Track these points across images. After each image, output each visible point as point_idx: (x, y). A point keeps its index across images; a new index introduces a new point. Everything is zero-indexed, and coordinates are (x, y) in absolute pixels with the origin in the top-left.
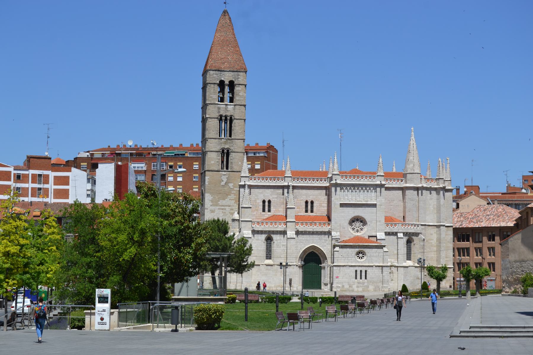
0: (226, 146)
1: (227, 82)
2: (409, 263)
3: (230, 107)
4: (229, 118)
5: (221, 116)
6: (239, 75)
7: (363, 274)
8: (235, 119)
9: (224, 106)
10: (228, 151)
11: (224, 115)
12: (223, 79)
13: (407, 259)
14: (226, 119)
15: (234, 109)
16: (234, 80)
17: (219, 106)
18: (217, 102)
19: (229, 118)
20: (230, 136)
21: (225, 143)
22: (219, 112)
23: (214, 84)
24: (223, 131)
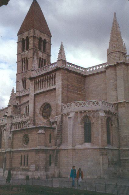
0: (25, 76)
1: (25, 38)
2: (87, 145)
3: (26, 52)
4: (26, 59)
5: (22, 59)
6: (30, 32)
7: (26, 159)
8: (28, 58)
9: (24, 53)
10: (25, 79)
11: (23, 58)
12: (23, 37)
13: (86, 141)
14: (25, 61)
15: (28, 53)
16: (28, 36)
17: (22, 54)
18: (20, 52)
19: (26, 59)
20: (27, 69)
21: (24, 75)
22: (22, 57)
23: (20, 42)
24: (24, 68)
